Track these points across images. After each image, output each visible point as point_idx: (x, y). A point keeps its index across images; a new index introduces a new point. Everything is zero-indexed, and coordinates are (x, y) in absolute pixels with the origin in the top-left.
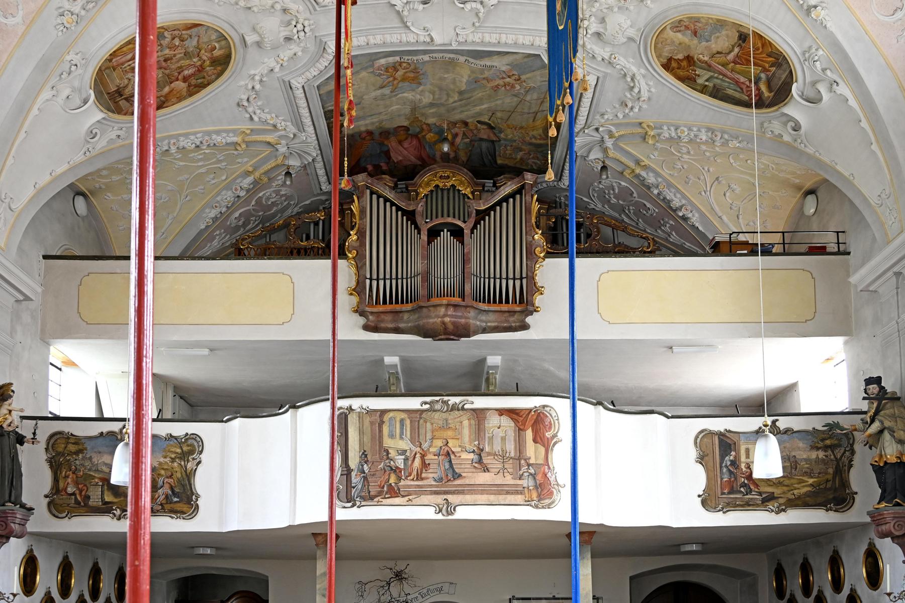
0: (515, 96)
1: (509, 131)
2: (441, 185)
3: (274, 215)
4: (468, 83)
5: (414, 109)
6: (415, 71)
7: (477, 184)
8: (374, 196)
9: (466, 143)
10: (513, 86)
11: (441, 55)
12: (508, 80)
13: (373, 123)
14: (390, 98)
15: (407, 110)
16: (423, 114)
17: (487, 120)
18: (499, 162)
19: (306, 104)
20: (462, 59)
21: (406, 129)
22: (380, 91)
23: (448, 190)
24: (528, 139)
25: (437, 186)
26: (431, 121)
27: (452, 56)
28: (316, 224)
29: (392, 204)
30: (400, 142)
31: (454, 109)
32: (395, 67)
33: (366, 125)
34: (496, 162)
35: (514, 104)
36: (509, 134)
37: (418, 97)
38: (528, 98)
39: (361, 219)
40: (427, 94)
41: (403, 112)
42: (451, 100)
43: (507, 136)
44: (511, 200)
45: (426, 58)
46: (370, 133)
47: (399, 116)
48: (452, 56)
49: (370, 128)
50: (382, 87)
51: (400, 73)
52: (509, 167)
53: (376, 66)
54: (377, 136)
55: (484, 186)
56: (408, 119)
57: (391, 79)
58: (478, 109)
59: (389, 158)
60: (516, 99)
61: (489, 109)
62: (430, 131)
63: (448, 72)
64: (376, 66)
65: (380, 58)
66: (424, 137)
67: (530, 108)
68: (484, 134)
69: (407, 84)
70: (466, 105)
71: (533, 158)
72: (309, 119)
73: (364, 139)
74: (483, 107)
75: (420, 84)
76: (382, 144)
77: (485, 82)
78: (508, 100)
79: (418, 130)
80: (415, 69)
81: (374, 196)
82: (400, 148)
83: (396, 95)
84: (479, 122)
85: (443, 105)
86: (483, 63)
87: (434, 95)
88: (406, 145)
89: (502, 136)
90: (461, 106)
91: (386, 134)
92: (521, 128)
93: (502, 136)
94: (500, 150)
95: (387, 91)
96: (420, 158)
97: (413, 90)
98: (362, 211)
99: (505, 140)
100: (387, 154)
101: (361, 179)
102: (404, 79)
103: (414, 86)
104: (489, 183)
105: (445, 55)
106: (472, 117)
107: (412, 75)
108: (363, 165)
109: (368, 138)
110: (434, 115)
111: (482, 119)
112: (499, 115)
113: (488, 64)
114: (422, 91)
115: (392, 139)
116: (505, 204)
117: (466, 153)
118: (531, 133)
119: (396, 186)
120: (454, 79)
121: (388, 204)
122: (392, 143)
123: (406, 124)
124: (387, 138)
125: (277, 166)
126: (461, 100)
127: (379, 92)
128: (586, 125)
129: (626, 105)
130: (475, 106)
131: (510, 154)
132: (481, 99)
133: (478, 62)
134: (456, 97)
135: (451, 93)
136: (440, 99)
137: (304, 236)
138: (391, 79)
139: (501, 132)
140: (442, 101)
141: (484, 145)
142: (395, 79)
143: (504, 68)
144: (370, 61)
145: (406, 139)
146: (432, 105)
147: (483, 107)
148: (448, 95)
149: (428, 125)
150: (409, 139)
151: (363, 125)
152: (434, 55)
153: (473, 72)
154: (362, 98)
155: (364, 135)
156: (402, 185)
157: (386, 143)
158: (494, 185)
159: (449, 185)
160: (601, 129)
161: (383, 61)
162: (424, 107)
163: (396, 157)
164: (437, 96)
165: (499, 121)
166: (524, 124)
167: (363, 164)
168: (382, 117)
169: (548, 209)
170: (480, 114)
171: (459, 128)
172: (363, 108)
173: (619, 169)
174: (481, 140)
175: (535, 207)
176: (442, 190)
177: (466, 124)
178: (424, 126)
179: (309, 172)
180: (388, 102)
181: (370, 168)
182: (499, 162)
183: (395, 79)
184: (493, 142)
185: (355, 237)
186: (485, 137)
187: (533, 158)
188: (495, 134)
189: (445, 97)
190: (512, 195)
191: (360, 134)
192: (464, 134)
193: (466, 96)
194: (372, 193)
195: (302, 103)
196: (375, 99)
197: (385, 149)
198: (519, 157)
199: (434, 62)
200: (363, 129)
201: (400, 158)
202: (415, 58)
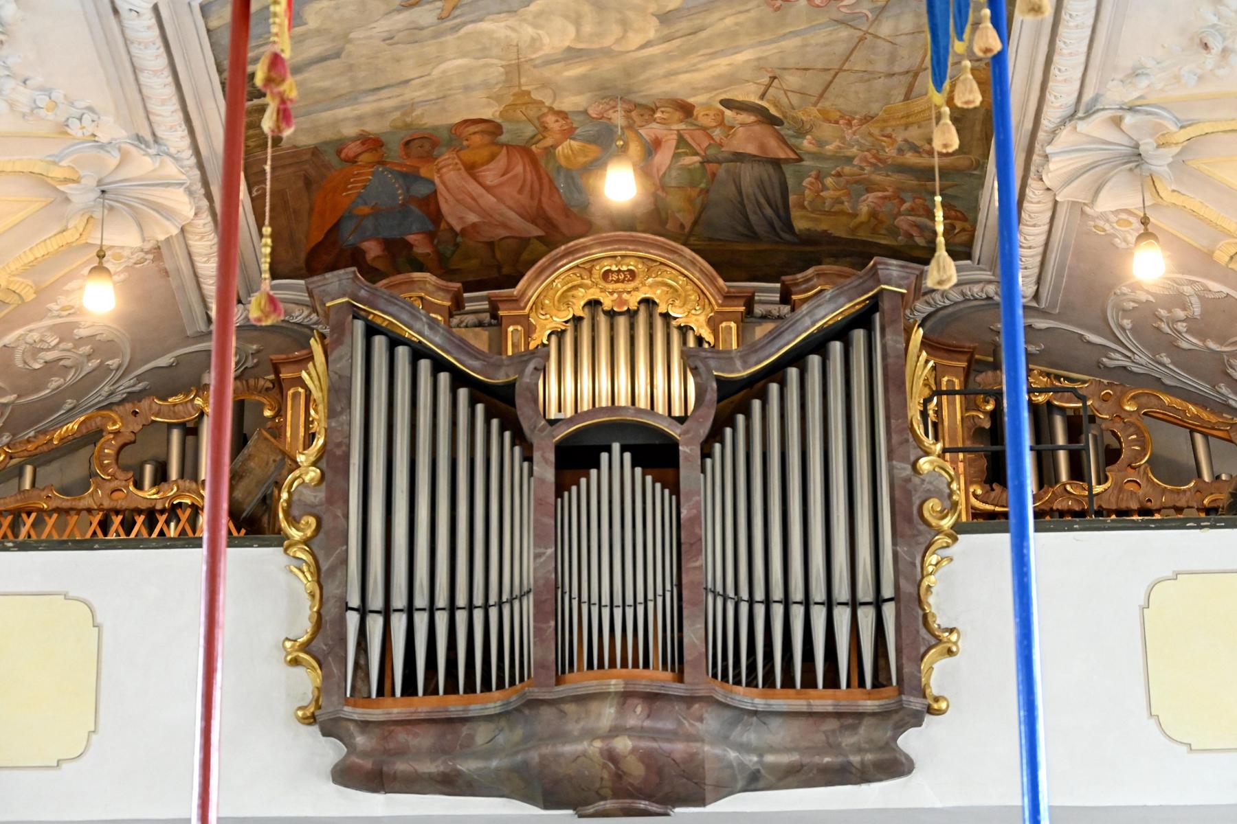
0: (842, 22)
1: (827, 130)
2: (608, 302)
3: (50, 405)
5: (515, 70)
7: (728, 297)
8: (379, 342)
9: (688, 169)
13: (381, 114)
15: (495, 71)
16: (545, 85)
17: (754, 99)
18: (800, 224)
19: (164, 61)
21: (492, 129)
23: (632, 315)
24: (891, 152)
25: (594, 304)
26: (570, 102)
28: (191, 431)
29: (439, 365)
30: (471, 169)
31: (647, 64)
33: (360, 119)
34: (789, 226)
35: (841, 48)
36: (832, 139)
37: (529, 31)
38: (885, 29)
39: (332, 414)
40: (558, 22)
41: (477, 79)
42: (635, 40)
43: (820, 143)
44: (836, 347)
46: (372, 143)
47: (467, 89)
49: (373, 127)
52: (836, 240)
54: (394, 151)
55: (750, 303)
56: (498, 98)
58: (722, 65)
59: (437, 216)
60: (844, 33)
61: (760, 65)
62: (569, 133)
66: (550, 151)
67: (892, 59)
68: (746, 137)
70: (685, 53)
71: (912, 211)
72: (174, 104)
73: (353, 161)
74: (740, 58)
76: (411, 177)
78: (821, 37)
79: (530, 131)
81: (379, 342)
82: (473, 187)
84: (727, 103)
85: (607, 52)
87: (577, 23)
88: (490, 175)
89: (806, 144)
90: (668, 57)
91: (424, 144)
92: (867, 119)
93: (806, 144)
94: (803, 189)
95: (425, 15)
96: (539, 217)
97: (512, 12)
98: (338, 392)
99: (817, 156)
100: (430, 206)
101: (338, 286)
104: (767, 293)
106: (707, 89)
108: (351, 240)
109: (366, 158)
110: (582, 84)
111: (739, 95)
112: (793, 80)
115: (447, 157)
116: (814, 360)
117: (690, 201)
118: (900, 137)
119: (458, 304)
121: (425, 365)
122: (448, 177)
123: (487, 114)
124: (429, 158)
125: (69, 250)
126: (667, 39)
127: (402, 19)
128: (1080, 110)
129: (1206, 46)
130: (713, 55)
131: (838, 201)
132: (732, 35)
134: (651, 30)
135: (631, 15)
137: (148, 470)
139: (801, 133)
140: (608, 42)
141: (748, 174)
145: (492, 157)
146: (573, 55)
147: (740, 58)
148: (625, 24)
149: (563, 115)
150: (502, 161)
151: (348, 119)
154: (346, 38)
155: (352, 149)
156: (477, 302)
157: (424, 172)
158: (785, 299)
159: (633, 301)
160: (1129, 119)
162: (549, 62)
163: (455, 215)
164: (587, 29)
165: (795, 99)
166: (875, 108)
167: (349, 237)
168: (410, 94)
169: (967, 373)
170: (732, 79)
171: (664, 122)
172: (350, 67)
173: (1200, 242)
174: (739, 157)
175: (920, 367)
176: (611, 314)
177: (686, 110)
178: (550, 120)
179: (169, 265)
180: (430, 48)
181: (372, 249)
182: (800, 224)
184: (776, 163)
185: (313, 474)
186: (751, 149)
187: (912, 211)
188: (783, 140)
189: (616, 31)
190: (841, 332)
191: (339, 145)
192: (681, 140)
193: (683, 26)
194: (372, 331)
195: (152, 58)
196: (389, 39)
197: (421, 190)
198: (864, 209)
200: (350, 131)
201: (473, 218)
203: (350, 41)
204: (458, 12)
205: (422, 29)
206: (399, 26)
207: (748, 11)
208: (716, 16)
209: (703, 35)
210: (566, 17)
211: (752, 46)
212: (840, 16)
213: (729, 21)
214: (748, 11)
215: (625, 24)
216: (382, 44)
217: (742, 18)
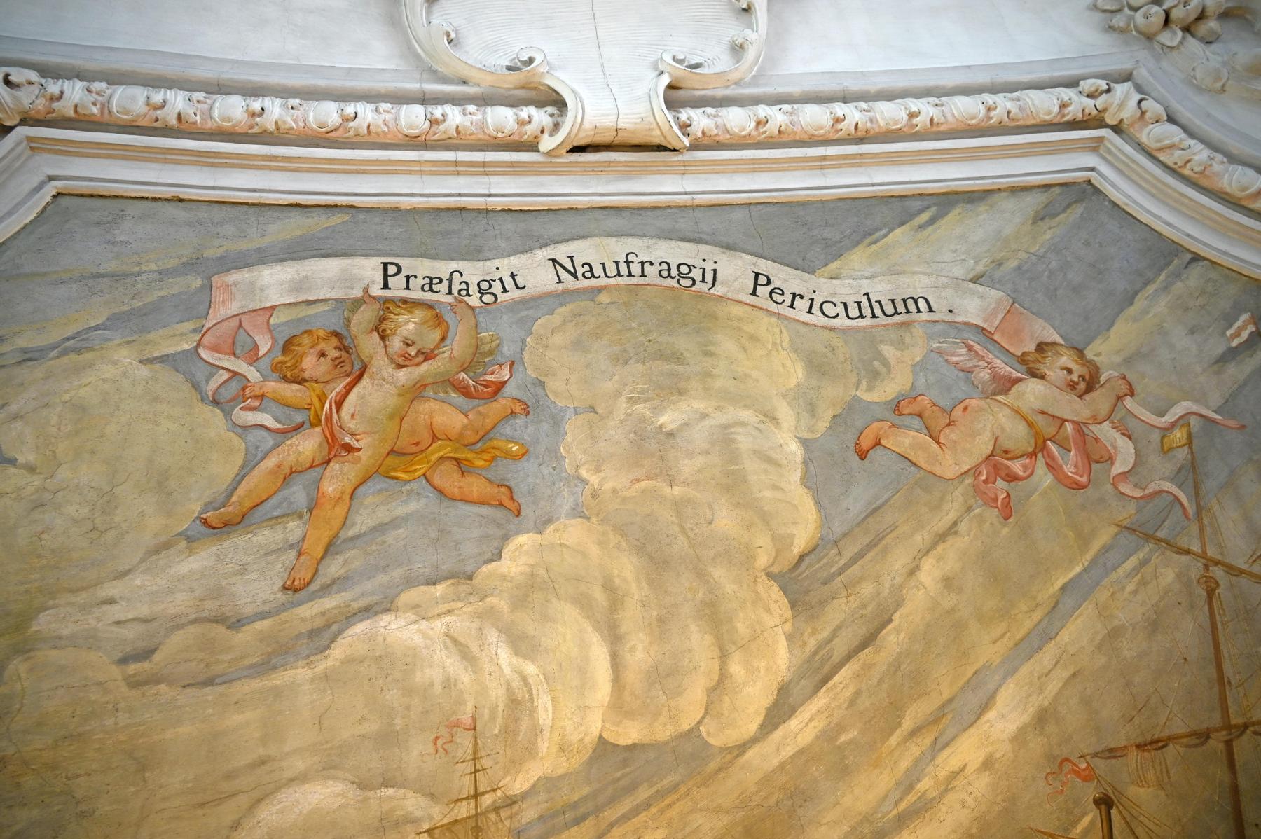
4: (820, 471)
6: (477, 383)
10: (1094, 456)
11: (618, 248)
12: (1032, 393)
14: (277, 655)
20: (735, 271)
22: (194, 564)
27: (676, 253)
32: (335, 347)
40: (571, 634)
42: (754, 696)
45: (535, 271)
48: (676, 253)
50: (221, 523)
51: (371, 399)
53: (226, 308)
57: (308, 445)
63: (675, 389)
64: (226, 308)
65: (262, 257)
69: (414, 503)
75: (508, 505)
77: (908, 439)
80: (479, 357)
83: (321, 636)
86: (846, 290)
102: (400, 458)
103: (469, 523)
105: (642, 249)
107: (448, 415)
113: (881, 290)
114: (530, 592)
120: (724, 439)
126: (818, 672)
133: (821, 286)
136: (665, 676)
138: (308, 445)
140: (690, 705)
142: (337, 448)
143: (974, 307)
144: (191, 266)
152: (584, 251)
153: (817, 366)
161: (274, 283)
164: (639, 653)
183: (337, 448)
199: (579, 292)
202: (473, 272)
203: (23, 649)
204: (334, 568)
205: (236, 624)
206: (180, 603)
207: (952, 530)
208: (899, 561)
209: (892, 640)
210: (583, 603)
211: (1010, 667)
212: (1126, 513)
213: (929, 574)
214: (952, 530)
215: (714, 616)
216: (116, 672)
217: (951, 552)
